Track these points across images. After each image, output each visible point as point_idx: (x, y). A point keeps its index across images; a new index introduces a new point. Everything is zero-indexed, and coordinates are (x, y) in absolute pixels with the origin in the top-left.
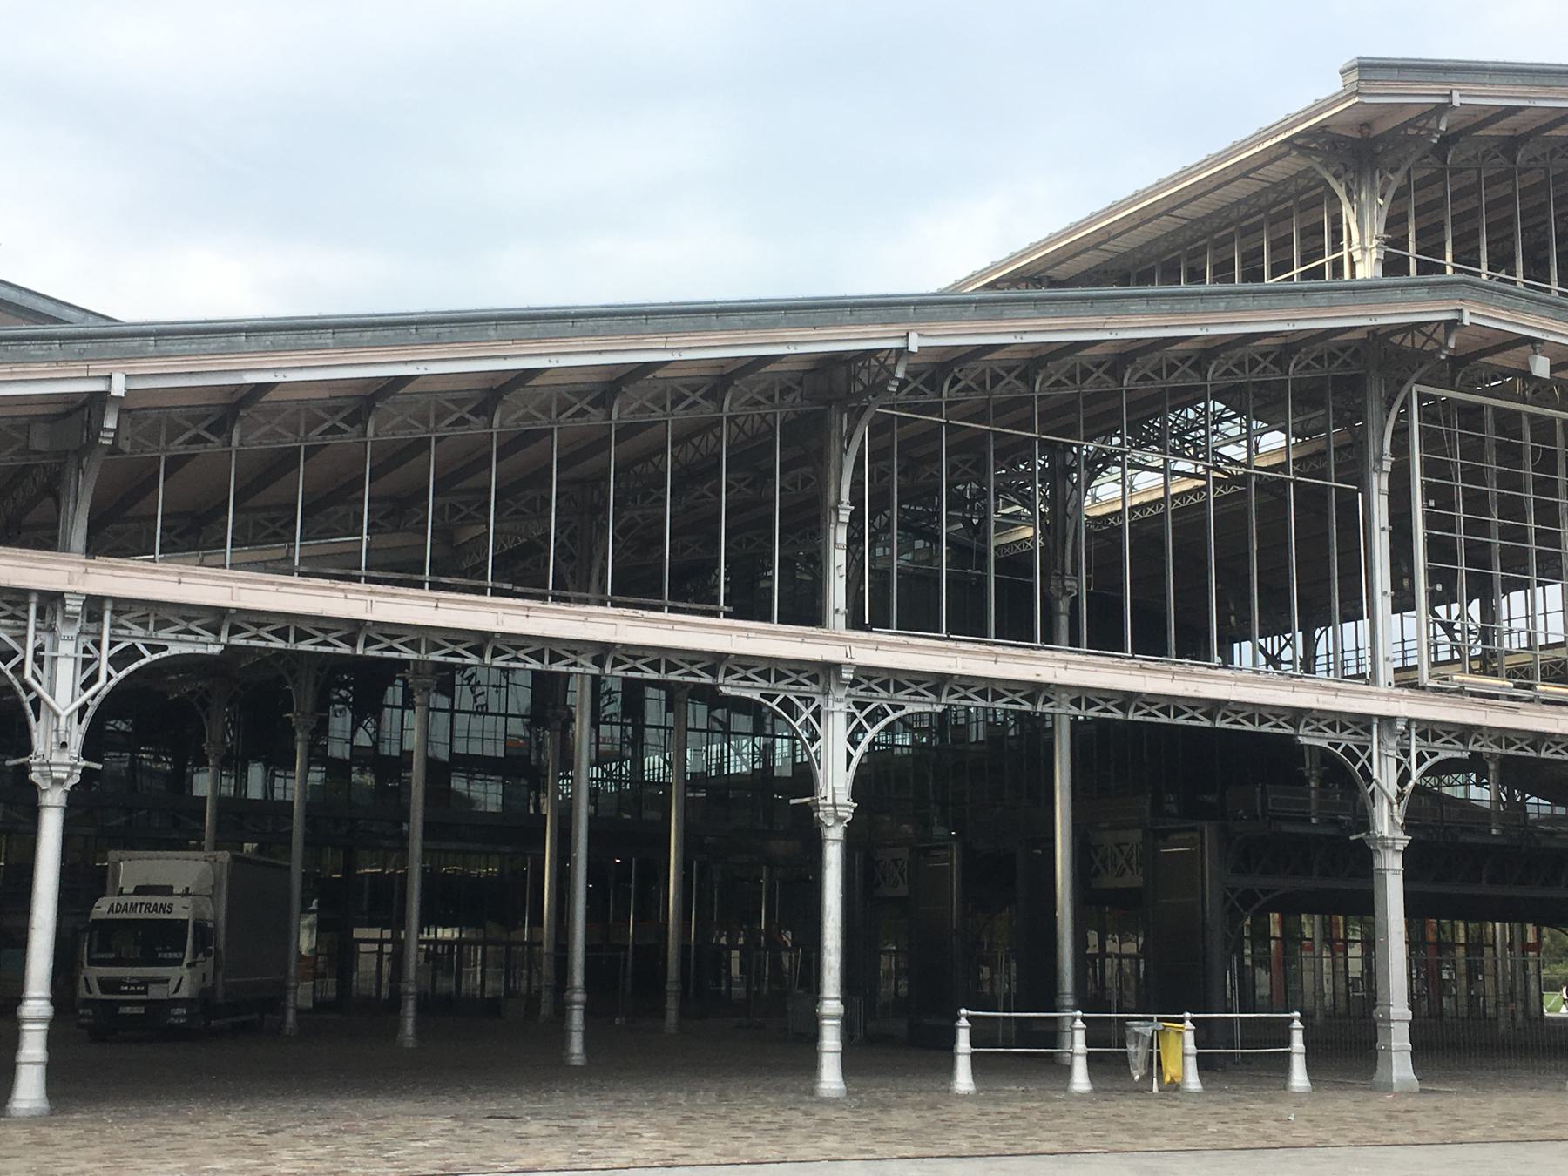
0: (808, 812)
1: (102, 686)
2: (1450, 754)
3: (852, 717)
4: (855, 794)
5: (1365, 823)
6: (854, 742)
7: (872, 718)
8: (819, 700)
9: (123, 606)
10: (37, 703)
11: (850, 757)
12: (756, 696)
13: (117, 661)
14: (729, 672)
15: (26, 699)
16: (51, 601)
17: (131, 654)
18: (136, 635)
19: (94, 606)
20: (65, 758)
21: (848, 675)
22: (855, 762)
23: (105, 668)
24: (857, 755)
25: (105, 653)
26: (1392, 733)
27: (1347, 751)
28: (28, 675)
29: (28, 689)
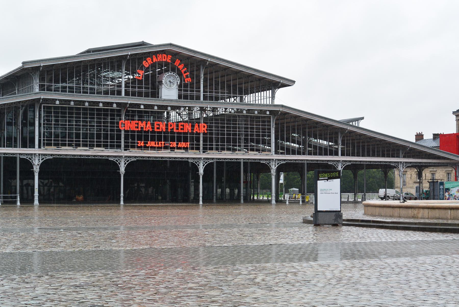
0: (119, 172)
1: (41, 162)
2: (211, 162)
3: (124, 161)
4: (125, 170)
5: (198, 171)
6: (125, 164)
7: (127, 162)
8: (120, 160)
9: (42, 154)
10: (34, 164)
11: (124, 166)
12: (112, 160)
13: (42, 160)
14: (110, 157)
15: (33, 164)
16: (35, 154)
17: (43, 159)
18: (44, 157)
19: (39, 154)
20: (37, 170)
21: (124, 157)
22: (125, 167)
23: (40, 160)
24: (125, 166)
25: (40, 159)
26: (402, 163)
27: (196, 162)
28: (33, 162)
29: (33, 163)
